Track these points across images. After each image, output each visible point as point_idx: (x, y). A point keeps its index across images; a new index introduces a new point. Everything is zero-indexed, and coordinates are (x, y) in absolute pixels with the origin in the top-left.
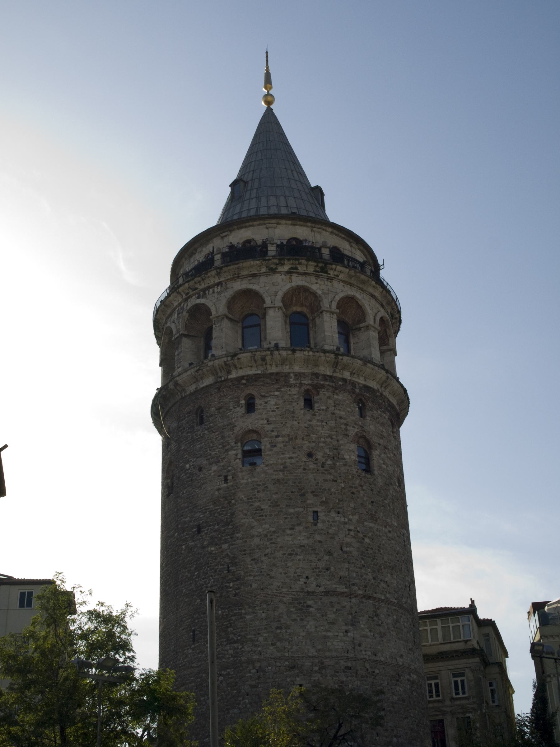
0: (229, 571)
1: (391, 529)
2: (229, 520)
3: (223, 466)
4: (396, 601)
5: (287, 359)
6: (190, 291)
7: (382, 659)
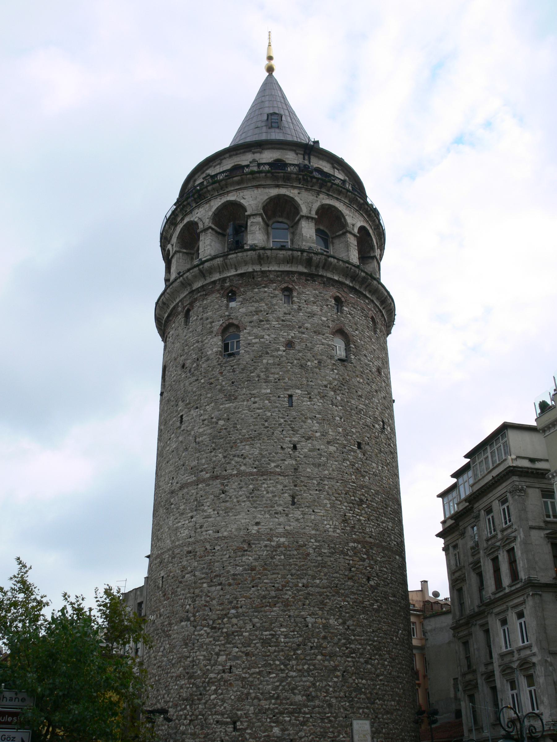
1: (257, 399)
4: (255, 470)
7: (225, 534)
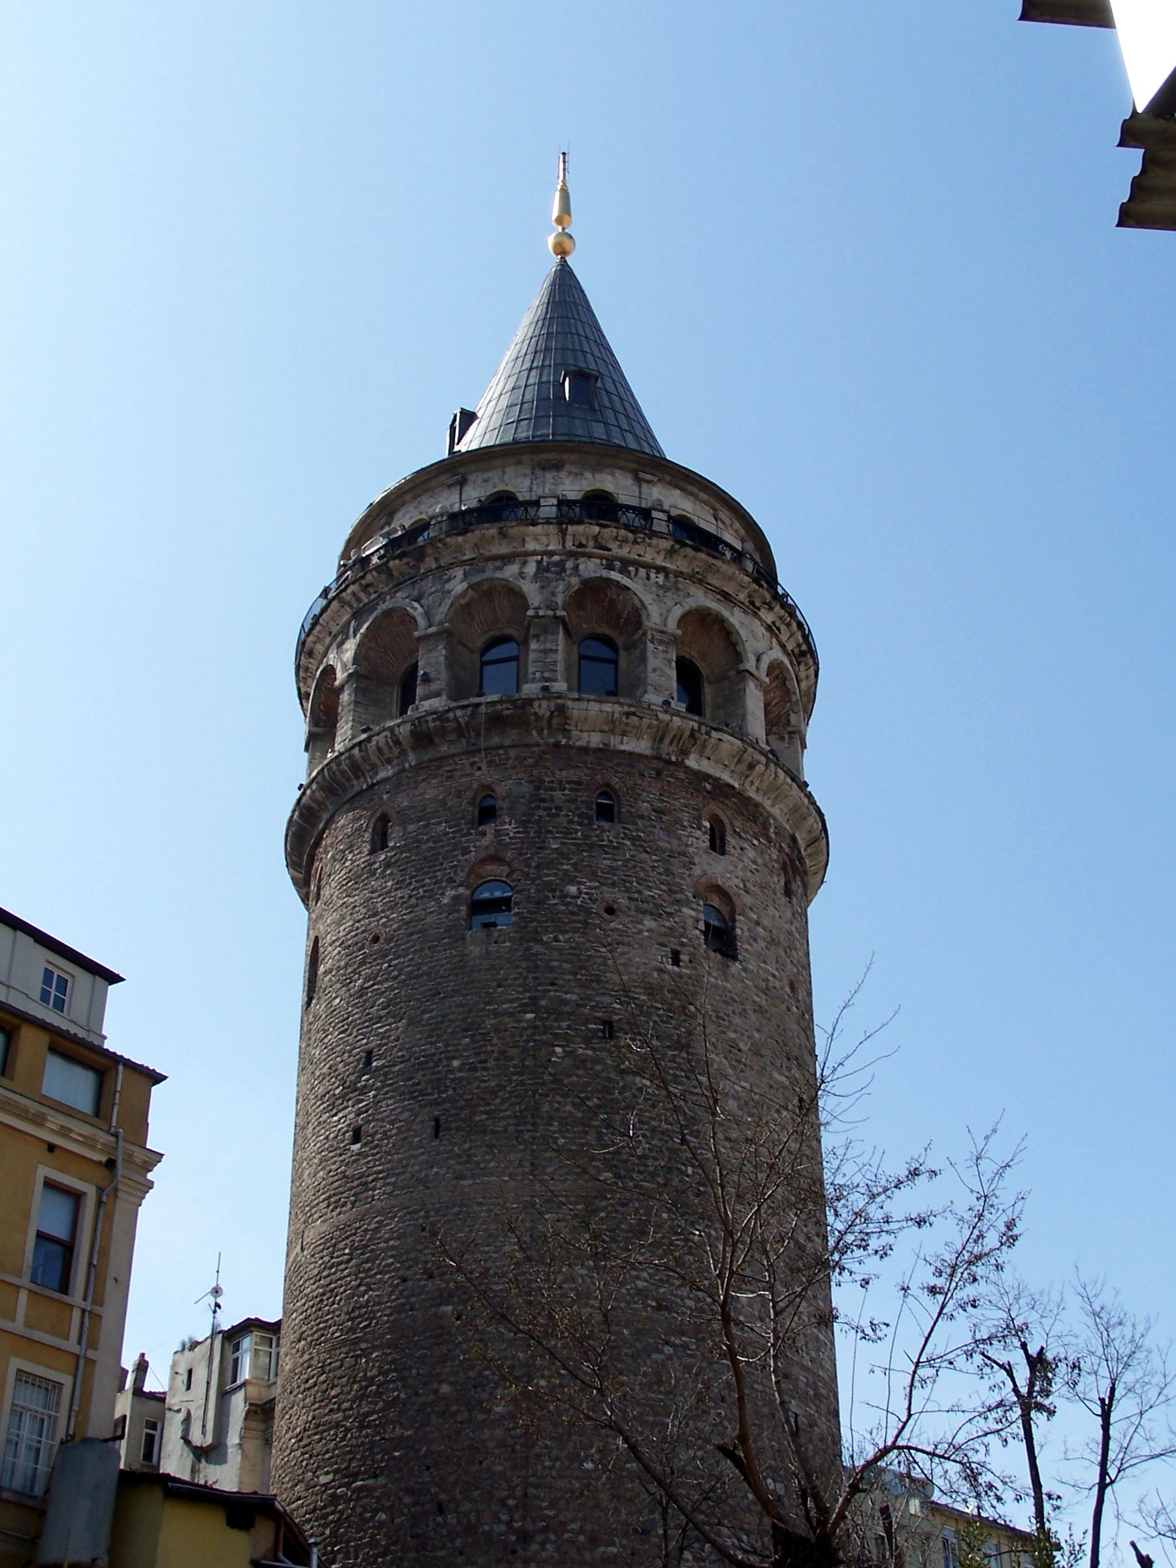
0: (684, 1141)
2: (683, 1041)
3: (670, 929)
5: (778, 788)
6: (591, 543)
